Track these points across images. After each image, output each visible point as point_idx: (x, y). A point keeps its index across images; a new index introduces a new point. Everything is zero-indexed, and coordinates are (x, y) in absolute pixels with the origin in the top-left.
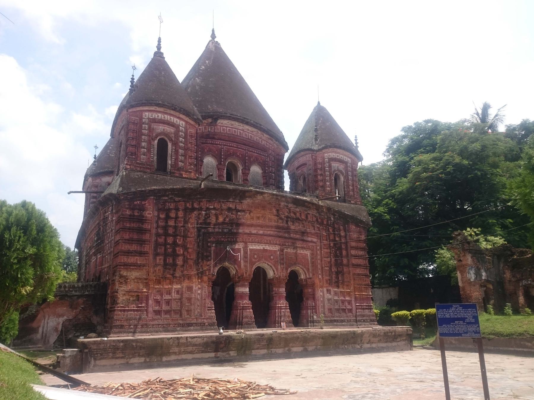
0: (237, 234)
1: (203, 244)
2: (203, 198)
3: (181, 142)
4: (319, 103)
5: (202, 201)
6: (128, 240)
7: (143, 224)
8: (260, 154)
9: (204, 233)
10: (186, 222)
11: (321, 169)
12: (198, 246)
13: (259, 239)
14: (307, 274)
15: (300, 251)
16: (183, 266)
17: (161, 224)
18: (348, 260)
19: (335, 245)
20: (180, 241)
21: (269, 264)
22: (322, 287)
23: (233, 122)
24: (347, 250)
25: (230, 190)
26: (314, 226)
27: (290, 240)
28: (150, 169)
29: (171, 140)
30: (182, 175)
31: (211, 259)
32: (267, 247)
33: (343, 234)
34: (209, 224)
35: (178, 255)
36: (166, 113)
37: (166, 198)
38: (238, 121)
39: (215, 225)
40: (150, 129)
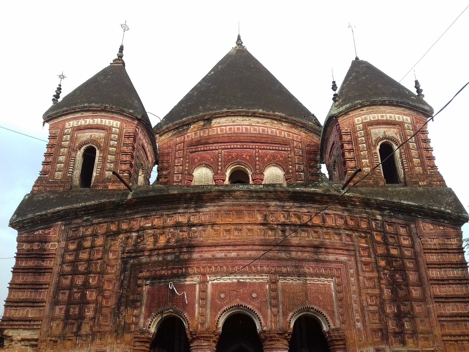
0: (190, 260)
1: (129, 282)
2: (136, 213)
3: (113, 146)
4: (357, 58)
5: (133, 219)
6: (20, 284)
7: (43, 261)
8: (279, 150)
9: (133, 265)
10: (106, 252)
11: (349, 142)
12: (121, 286)
13: (229, 266)
14: (330, 321)
15: (311, 281)
17: (69, 258)
18: (424, 291)
19: (389, 263)
20: (94, 280)
21: (250, 307)
23: (234, 119)
24: (417, 269)
25: (174, 195)
26: (340, 234)
27: (290, 263)
28: (64, 187)
29: (99, 147)
30: (107, 187)
31: (141, 305)
32: (245, 278)
33: (406, 243)
34: (143, 251)
35: (88, 303)
36: (96, 117)
37: (79, 221)
38: (241, 116)
39: (151, 250)
40: (72, 140)
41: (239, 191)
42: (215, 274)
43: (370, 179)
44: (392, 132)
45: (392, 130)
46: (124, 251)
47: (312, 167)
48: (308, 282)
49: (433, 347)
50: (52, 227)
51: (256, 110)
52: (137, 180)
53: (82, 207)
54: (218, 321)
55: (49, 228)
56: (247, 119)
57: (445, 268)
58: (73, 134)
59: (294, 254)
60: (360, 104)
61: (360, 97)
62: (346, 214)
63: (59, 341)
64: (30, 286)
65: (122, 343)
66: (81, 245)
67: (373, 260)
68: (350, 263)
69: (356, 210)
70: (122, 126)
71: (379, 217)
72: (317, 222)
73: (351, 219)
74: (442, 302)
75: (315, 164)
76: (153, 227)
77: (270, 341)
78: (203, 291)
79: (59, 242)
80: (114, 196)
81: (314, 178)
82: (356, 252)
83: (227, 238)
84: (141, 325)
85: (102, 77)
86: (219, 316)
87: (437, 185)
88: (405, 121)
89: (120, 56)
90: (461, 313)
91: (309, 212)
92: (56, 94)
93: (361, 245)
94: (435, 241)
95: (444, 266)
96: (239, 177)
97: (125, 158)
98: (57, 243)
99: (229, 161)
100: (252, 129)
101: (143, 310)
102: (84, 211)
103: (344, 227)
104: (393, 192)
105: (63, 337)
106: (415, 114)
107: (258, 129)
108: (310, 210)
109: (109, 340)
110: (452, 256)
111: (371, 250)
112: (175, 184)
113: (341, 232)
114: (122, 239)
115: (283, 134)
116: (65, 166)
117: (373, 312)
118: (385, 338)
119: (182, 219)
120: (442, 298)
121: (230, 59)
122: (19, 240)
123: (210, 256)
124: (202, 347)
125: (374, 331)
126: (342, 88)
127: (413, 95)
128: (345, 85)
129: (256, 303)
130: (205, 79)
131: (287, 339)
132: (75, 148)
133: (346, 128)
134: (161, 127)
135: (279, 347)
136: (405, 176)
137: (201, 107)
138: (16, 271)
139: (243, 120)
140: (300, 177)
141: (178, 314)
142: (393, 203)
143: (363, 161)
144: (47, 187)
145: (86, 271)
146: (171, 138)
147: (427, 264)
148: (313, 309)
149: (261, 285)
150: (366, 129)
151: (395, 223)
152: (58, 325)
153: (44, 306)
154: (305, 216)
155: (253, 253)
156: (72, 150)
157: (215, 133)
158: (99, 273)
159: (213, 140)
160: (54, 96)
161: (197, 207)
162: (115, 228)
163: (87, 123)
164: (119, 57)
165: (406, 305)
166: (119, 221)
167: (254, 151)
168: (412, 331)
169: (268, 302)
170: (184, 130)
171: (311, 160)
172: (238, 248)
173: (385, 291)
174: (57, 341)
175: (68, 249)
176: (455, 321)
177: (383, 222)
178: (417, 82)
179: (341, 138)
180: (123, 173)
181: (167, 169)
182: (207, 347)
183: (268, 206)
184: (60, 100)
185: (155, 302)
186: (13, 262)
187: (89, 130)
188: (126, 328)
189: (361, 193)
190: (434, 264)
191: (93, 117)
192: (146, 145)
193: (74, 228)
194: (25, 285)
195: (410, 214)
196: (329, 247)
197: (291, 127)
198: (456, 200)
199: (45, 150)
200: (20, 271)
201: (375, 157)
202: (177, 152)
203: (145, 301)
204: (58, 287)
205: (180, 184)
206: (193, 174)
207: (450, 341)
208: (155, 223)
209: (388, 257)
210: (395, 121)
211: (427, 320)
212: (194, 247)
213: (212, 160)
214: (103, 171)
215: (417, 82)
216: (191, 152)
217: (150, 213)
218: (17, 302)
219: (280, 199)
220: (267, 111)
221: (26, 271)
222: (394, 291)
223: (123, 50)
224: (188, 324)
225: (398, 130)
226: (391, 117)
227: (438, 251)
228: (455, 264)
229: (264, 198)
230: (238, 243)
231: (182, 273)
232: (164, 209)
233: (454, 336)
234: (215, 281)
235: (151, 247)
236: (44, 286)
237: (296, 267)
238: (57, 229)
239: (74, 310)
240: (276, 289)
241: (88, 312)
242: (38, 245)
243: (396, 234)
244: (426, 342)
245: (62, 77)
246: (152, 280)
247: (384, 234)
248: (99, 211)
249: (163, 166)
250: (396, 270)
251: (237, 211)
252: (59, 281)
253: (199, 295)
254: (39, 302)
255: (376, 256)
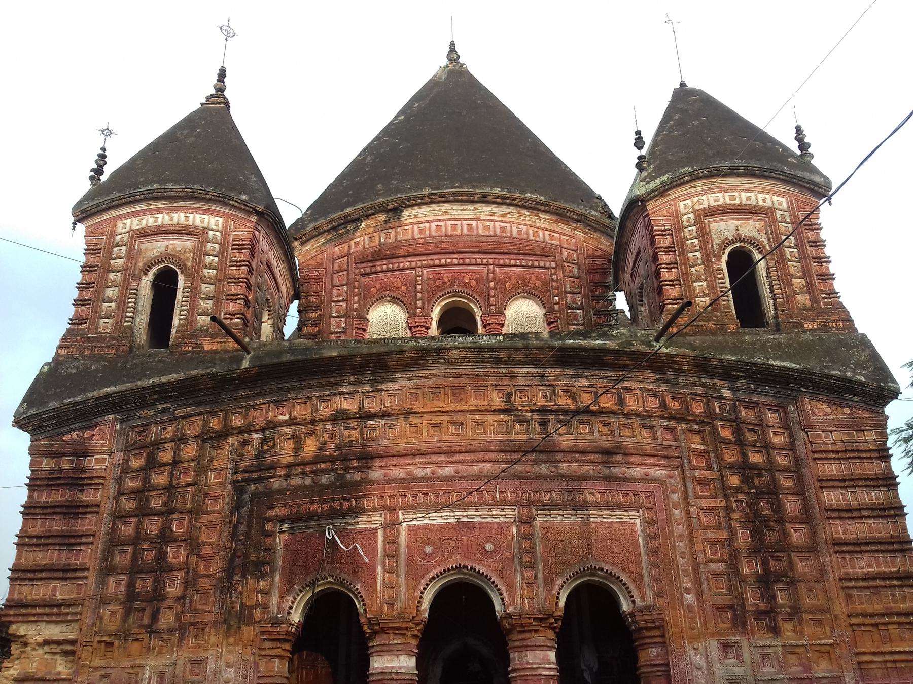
0: (364, 482)
1: (249, 527)
2: (259, 395)
3: (210, 267)
4: (683, 85)
5: (253, 407)
6: (39, 537)
7: (82, 491)
9: (255, 496)
10: (202, 470)
11: (669, 250)
12: (234, 535)
13: (437, 493)
14: (635, 593)
15: (597, 517)
16: (183, 597)
18: (813, 532)
19: (746, 480)
20: (180, 525)
21: (482, 569)
22: (700, 637)
23: (445, 207)
24: (801, 491)
26: (652, 427)
27: (556, 484)
29: (184, 268)
30: (201, 346)
31: (273, 571)
32: (472, 515)
33: (779, 440)
34: (273, 467)
35: (171, 569)
36: (177, 210)
37: (149, 413)
38: (458, 201)
39: (289, 466)
40: (131, 256)
41: (456, 348)
42: (414, 508)
43: (709, 320)
44: (751, 228)
45: (752, 223)
46: (236, 468)
47: (597, 299)
48: (592, 520)
49: (830, 638)
50: (96, 426)
51: (488, 190)
52: (258, 331)
53: (154, 386)
54: (421, 597)
55: (91, 428)
56: (471, 207)
57: (854, 487)
58: (131, 244)
59: (564, 467)
60: (690, 174)
61: (688, 161)
62: (663, 387)
63: (116, 644)
64: (57, 540)
65: (238, 645)
66: (154, 459)
67: (715, 474)
68: (672, 481)
69: (683, 380)
70: (226, 227)
71: (727, 393)
72: (608, 405)
73: (674, 398)
74: (848, 552)
75: (604, 292)
76: (291, 422)
77: (520, 632)
78: (392, 541)
79: (111, 453)
80: (215, 364)
81: (603, 319)
82: (683, 461)
83: (436, 438)
84: (274, 608)
85: (185, 132)
86: (422, 587)
87: (837, 329)
88: (776, 206)
89: (220, 90)
90: (884, 572)
91: (592, 386)
92: (96, 166)
93: (693, 446)
94: (835, 436)
95: (851, 483)
96: (457, 321)
97: (234, 289)
98: (107, 457)
99: (437, 289)
100: (480, 226)
101: (277, 580)
102: (157, 393)
103: (659, 413)
104: (753, 344)
105: (125, 635)
106: (795, 191)
107: (491, 226)
108: (595, 381)
109: (213, 639)
110: (866, 464)
111: (712, 455)
112: (333, 337)
113: (655, 422)
114: (233, 445)
115: (541, 235)
116: (118, 307)
117: (717, 575)
118: (739, 622)
119: (349, 405)
120: (847, 544)
121: (436, 89)
122: (33, 452)
123: (403, 475)
124: (391, 648)
125: (720, 609)
126: (655, 143)
127: (793, 155)
128: (659, 138)
129: (493, 562)
130: (386, 131)
131: (553, 629)
132: (137, 272)
133: (663, 222)
134: (304, 227)
135: (538, 644)
136: (776, 313)
137: (380, 187)
138: (29, 511)
139: (462, 210)
140: (576, 318)
141: (344, 587)
142: (754, 364)
143: (696, 284)
144: (85, 347)
145: (164, 509)
146: (323, 248)
147: (820, 481)
148: (602, 570)
149: (503, 527)
150: (701, 223)
151: (757, 403)
152: (113, 613)
153: (86, 577)
154: (585, 394)
155: (487, 467)
156: (131, 275)
157: (410, 237)
158: (190, 512)
159: (405, 249)
160: (92, 170)
161: (376, 381)
162: (218, 424)
163: (159, 223)
164: (217, 90)
165: (778, 559)
166: (226, 412)
167: (486, 269)
168: (790, 607)
169: (516, 560)
170: (348, 232)
171: (597, 284)
172: (457, 457)
173: (740, 533)
174: (112, 644)
175: (128, 467)
176: (873, 587)
177: (735, 404)
178: (799, 130)
179: (653, 241)
180: (231, 319)
181: (316, 308)
182: (400, 648)
183: (513, 377)
184: (104, 178)
185: (300, 564)
186: (23, 495)
187: (164, 236)
188: (245, 616)
189: (693, 348)
190: (832, 480)
191: (170, 210)
192: (274, 262)
193: (140, 426)
194: (49, 537)
195: (786, 385)
196: (632, 451)
197: (556, 222)
198: (875, 357)
199: (79, 277)
200: (37, 511)
201: (719, 276)
202: (336, 275)
203: (279, 563)
204: (111, 540)
205: (343, 337)
206: (368, 317)
207: (864, 625)
208: (295, 413)
209: (744, 468)
210: (757, 205)
211: (818, 586)
212: (372, 458)
213: (404, 288)
214: (192, 315)
215: (799, 130)
216: (363, 275)
217: (286, 395)
218: (34, 571)
219: (535, 363)
220: (509, 191)
221: (49, 511)
222: (756, 534)
223: (224, 76)
224: (364, 605)
225: (763, 224)
226: (748, 199)
227: (840, 455)
228: (873, 479)
229: (505, 361)
230: (458, 448)
231: (350, 508)
232: (312, 387)
233: (872, 615)
234: (415, 522)
235: (289, 459)
236: (84, 540)
237: (568, 491)
238: (107, 428)
239: (145, 584)
240: (531, 534)
241: (171, 586)
242: (71, 462)
243: (760, 425)
244: (819, 629)
245: (107, 132)
246: (293, 522)
247: (737, 425)
248: (185, 392)
249: (310, 302)
250: (760, 494)
251: (453, 388)
252: (112, 529)
253: (384, 549)
254: (75, 570)
255: (722, 467)
